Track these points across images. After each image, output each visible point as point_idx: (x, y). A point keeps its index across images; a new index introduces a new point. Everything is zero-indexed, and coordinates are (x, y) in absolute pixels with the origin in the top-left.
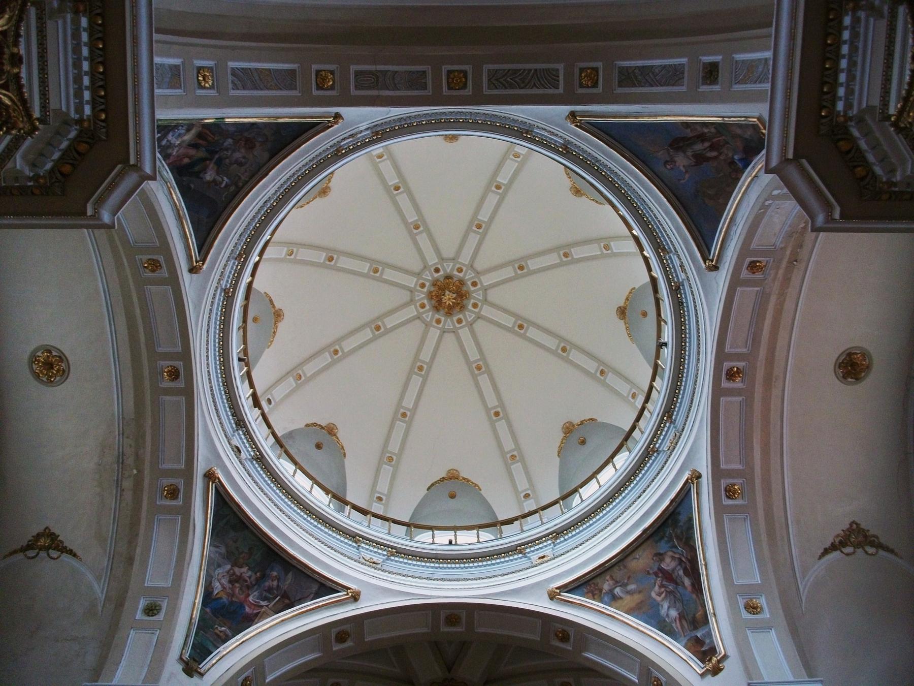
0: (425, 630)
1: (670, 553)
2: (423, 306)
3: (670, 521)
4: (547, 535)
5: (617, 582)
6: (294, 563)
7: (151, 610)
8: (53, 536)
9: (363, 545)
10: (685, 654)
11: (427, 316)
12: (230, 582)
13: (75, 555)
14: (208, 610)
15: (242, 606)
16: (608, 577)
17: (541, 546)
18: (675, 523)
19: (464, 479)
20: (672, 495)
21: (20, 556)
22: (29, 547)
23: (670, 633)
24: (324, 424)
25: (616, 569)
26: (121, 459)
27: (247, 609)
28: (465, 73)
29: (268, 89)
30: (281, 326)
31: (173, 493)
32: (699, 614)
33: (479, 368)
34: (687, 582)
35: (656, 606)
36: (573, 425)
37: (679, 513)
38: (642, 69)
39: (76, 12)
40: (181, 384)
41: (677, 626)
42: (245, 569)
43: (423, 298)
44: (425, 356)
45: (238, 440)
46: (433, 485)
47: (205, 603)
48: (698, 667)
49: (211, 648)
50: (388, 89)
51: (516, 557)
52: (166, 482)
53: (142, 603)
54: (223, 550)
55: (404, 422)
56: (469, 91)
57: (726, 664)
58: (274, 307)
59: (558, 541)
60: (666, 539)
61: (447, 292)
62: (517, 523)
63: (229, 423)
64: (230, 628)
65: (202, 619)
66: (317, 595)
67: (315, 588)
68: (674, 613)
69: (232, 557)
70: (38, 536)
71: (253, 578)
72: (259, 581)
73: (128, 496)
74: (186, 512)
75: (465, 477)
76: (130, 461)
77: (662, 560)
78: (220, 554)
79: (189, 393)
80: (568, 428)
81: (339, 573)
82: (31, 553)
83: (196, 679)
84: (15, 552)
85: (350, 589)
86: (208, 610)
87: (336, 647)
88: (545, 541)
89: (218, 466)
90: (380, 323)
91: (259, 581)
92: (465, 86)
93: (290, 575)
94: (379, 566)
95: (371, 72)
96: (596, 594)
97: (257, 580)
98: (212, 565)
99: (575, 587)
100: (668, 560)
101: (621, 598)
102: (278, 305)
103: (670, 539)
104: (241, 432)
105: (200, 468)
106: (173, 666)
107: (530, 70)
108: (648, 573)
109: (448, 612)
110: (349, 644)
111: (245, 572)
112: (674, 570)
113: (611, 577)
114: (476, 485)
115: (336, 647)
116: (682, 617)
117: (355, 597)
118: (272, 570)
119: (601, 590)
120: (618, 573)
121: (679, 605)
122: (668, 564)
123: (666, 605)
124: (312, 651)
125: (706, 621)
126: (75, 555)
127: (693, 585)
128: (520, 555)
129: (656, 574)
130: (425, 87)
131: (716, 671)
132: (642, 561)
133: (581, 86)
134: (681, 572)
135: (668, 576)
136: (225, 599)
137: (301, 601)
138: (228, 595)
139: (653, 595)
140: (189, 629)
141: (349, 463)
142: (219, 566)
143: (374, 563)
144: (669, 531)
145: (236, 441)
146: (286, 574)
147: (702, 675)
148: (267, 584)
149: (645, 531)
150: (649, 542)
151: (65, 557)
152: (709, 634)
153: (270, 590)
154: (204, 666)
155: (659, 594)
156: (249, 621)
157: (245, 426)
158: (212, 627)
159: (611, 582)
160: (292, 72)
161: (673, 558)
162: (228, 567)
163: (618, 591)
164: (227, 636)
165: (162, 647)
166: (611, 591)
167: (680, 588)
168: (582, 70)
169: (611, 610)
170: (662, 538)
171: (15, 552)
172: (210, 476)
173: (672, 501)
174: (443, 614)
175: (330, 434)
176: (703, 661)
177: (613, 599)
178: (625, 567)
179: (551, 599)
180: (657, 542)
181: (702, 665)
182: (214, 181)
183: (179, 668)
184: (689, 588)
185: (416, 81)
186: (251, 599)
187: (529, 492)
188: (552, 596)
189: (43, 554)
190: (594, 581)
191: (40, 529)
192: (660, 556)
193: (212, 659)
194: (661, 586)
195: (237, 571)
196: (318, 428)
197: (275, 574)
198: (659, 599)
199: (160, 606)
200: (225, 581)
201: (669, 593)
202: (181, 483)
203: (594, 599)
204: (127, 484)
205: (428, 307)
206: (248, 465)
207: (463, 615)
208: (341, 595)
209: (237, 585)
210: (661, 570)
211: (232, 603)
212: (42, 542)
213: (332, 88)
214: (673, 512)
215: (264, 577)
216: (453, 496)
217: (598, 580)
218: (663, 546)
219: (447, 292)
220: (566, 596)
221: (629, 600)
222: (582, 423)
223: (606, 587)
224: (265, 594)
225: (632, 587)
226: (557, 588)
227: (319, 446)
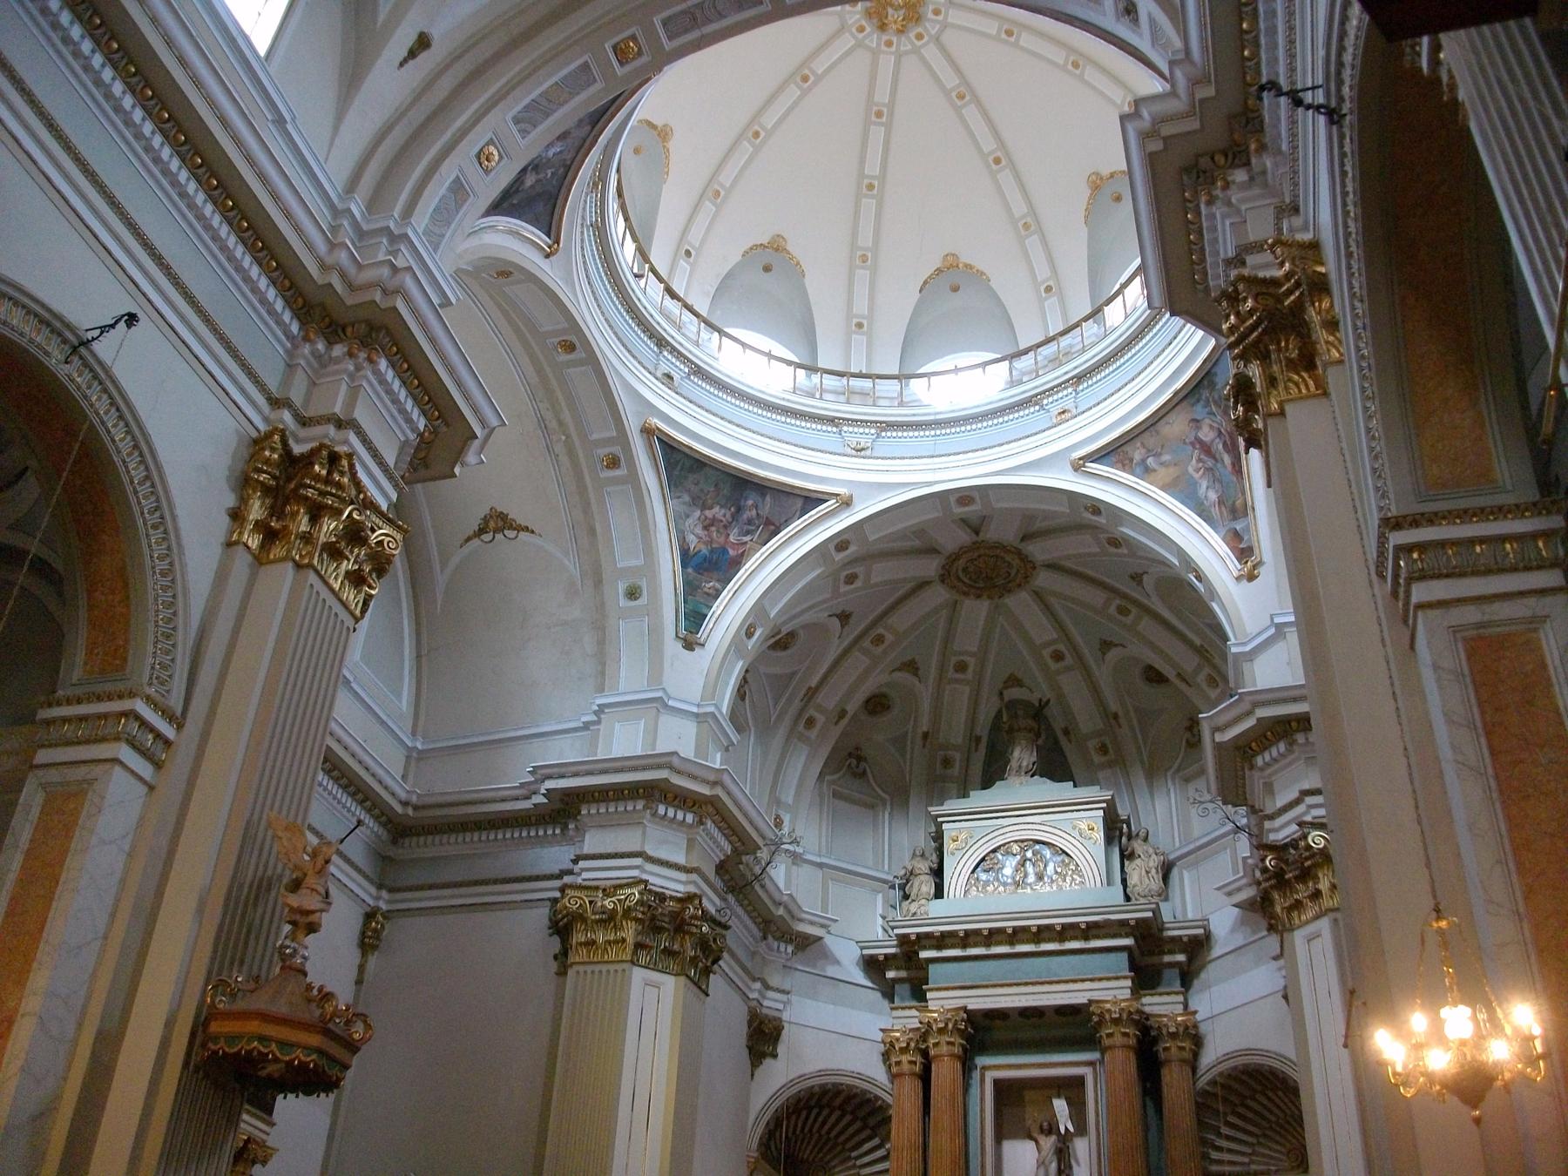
0: (936, 515)
1: (1207, 421)
2: (861, 29)
3: (1206, 383)
4: (1068, 381)
5: (1149, 451)
6: (768, 484)
7: (633, 594)
8: (502, 517)
9: (845, 428)
10: (1224, 549)
11: (872, 41)
12: (706, 528)
13: (533, 532)
14: (690, 570)
15: (724, 550)
16: (1139, 444)
17: (1060, 395)
18: (1212, 385)
19: (966, 266)
20: (1205, 354)
21: (476, 542)
22: (482, 531)
23: (1208, 519)
24: (765, 242)
25: (1147, 434)
26: (542, 423)
27: (732, 552)
29: (561, 105)
30: (671, 145)
31: (614, 463)
32: (1239, 502)
33: (961, 97)
34: (1227, 459)
35: (1194, 485)
36: (1101, 178)
37: (1216, 374)
39: (370, 360)
40: (579, 354)
41: (1215, 512)
42: (717, 509)
43: (859, 20)
44: (882, 96)
45: (668, 363)
46: (925, 283)
47: (684, 565)
48: (1234, 565)
49: (705, 611)
50: (711, 21)
51: (1032, 410)
52: (603, 452)
53: (622, 588)
54: (687, 498)
55: (873, 197)
57: (1262, 570)
58: (654, 127)
59: (1081, 387)
60: (1202, 403)
61: (890, 11)
62: (1031, 354)
63: (646, 347)
64: (718, 581)
65: (687, 583)
66: (804, 512)
67: (799, 503)
68: (1213, 496)
69: (699, 502)
70: (486, 520)
71: (728, 515)
72: (735, 517)
73: (564, 459)
74: (634, 478)
75: (968, 262)
76: (553, 424)
77: (1199, 428)
78: (684, 503)
79: (592, 361)
80: (1094, 182)
81: (822, 480)
82: (487, 537)
83: (698, 649)
84: (468, 539)
85: (838, 495)
86: (690, 570)
87: (839, 557)
88: (1065, 388)
89: (653, 416)
90: (806, 71)
91: (735, 517)
93: (768, 498)
94: (868, 453)
95: (683, 12)
96: (1126, 464)
97: (733, 516)
98: (679, 520)
99: (1101, 456)
100: (1206, 429)
101: (1155, 471)
102: (659, 122)
103: (1207, 404)
104: (665, 353)
105: (633, 425)
106: (673, 647)
108: (1185, 443)
109: (957, 495)
110: (852, 549)
111: (718, 512)
112: (1213, 441)
113: (1143, 445)
114: (983, 273)
115: (839, 557)
116: (1221, 502)
117: (847, 503)
118: (746, 499)
119: (1131, 460)
120: (1150, 439)
121: (1217, 485)
122: (1206, 434)
123: (1204, 484)
124: (813, 570)
125: (1246, 515)
126: (533, 532)
127: (1233, 465)
128: (1037, 408)
129: (1192, 444)
131: (1251, 577)
132: (1177, 425)
134: (1220, 446)
135: (1206, 449)
136: (705, 550)
137: (787, 523)
138: (706, 543)
139: (1190, 470)
140: (677, 602)
141: (812, 283)
142: (688, 516)
143: (863, 449)
144: (1205, 393)
145: (664, 367)
146: (763, 495)
147: (1238, 579)
148: (745, 516)
149: (1176, 393)
150: (1184, 404)
151: (522, 535)
152: (1247, 529)
153: (750, 522)
154: (702, 634)
155: (1197, 470)
156: (737, 563)
157: (668, 343)
158: (699, 587)
159: (1143, 451)
160: (585, 66)
161: (1211, 427)
162: (698, 513)
163: (1150, 461)
164: (717, 590)
165: (655, 632)
166: (1144, 461)
167: (1219, 465)
169: (1143, 485)
170: (1198, 401)
171: (468, 539)
172: (648, 431)
173: (1205, 361)
174: (952, 499)
175: (777, 250)
176: (1239, 560)
177: (1146, 472)
178: (1157, 432)
179: (1076, 470)
180: (1193, 405)
181: (1239, 567)
182: (538, 181)
183: (679, 645)
184: (1229, 467)
186: (732, 538)
187: (1051, 283)
188: (1078, 466)
189: (499, 536)
190: (1124, 448)
191: (484, 511)
192: (1196, 422)
193: (708, 624)
194: (1200, 460)
195: (709, 513)
197: (750, 502)
198: (1196, 476)
199: (640, 587)
200: (699, 531)
201: (1209, 470)
202: (617, 450)
203: (1124, 471)
204: (559, 448)
205: (868, 29)
206: (687, 384)
207: (976, 495)
208: (831, 504)
209: (713, 529)
210: (1201, 442)
211: (712, 551)
212: (492, 524)
213: (640, 53)
214: (1208, 373)
215: (739, 510)
216: (955, 289)
217: (1127, 448)
218: (1199, 411)
219: (890, 11)
220: (1094, 467)
221: (1164, 474)
222: (1112, 175)
223: (1137, 457)
224: (745, 527)
225: (1166, 457)
226: (1080, 459)
227: (767, 269)
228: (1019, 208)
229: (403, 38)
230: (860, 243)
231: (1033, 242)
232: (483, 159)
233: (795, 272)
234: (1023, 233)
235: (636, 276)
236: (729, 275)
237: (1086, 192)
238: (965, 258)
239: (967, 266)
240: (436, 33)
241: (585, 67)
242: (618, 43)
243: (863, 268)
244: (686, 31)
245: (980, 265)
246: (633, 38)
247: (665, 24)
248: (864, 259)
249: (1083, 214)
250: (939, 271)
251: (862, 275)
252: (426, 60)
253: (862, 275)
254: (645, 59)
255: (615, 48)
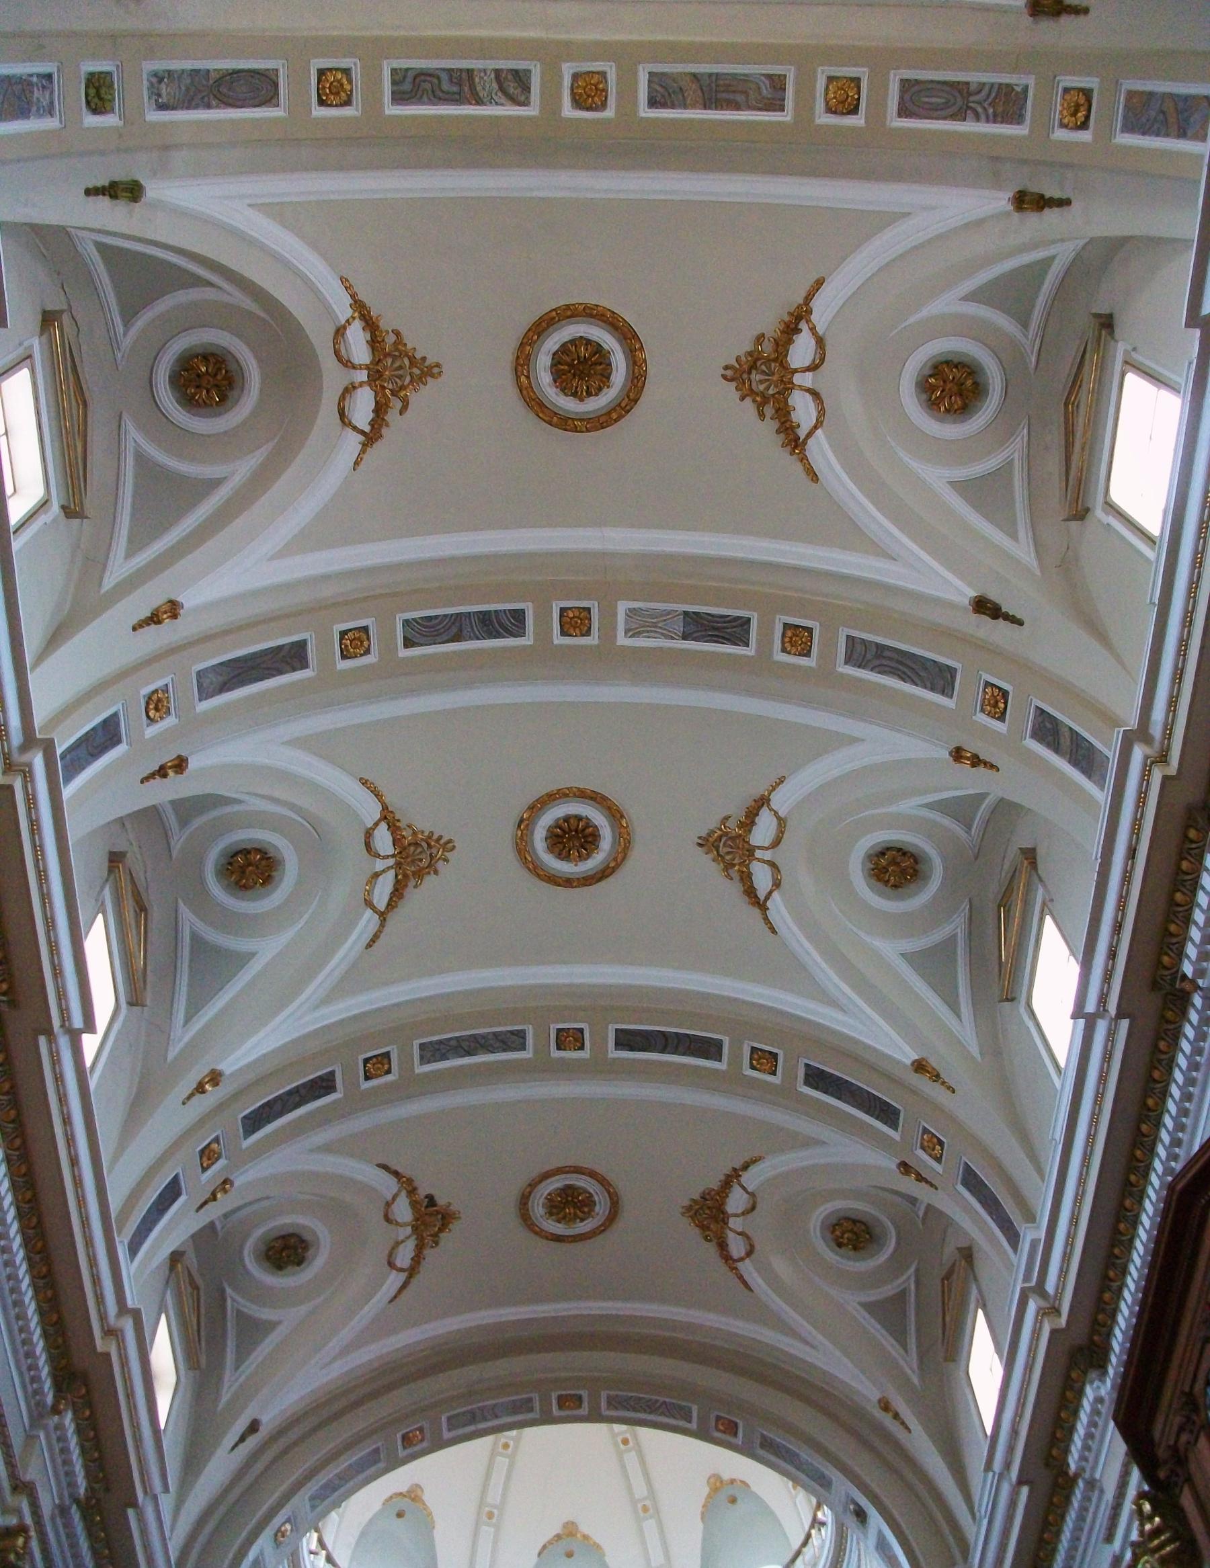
28: (580, 1398)
36: (722, 1482)
38: (788, 1450)
46: (544, 1547)
56: (584, 1410)
75: (586, 1533)
92: (580, 1406)
107: (657, 1401)
114: (598, 1547)
130: (531, 1410)
133: (718, 1430)
168: (718, 1418)
175: (413, 1500)
185: (524, 1406)
196: (399, 1498)
213: (422, 1440)
216: (570, 1555)
222: (732, 1481)
227: (400, 1515)
228: (640, 1490)
229: (241, 1425)
230: (489, 1500)
231: (650, 1525)
232: (280, 1534)
233: (427, 1524)
234: (642, 1514)
235: (311, 1552)
236: (371, 1521)
237: (706, 1490)
238: (584, 1528)
239: (586, 1537)
240: (265, 1419)
241: (377, 1451)
242: (408, 1433)
243: (488, 1525)
244: (465, 1425)
245: (597, 1538)
246: (421, 1429)
247: (449, 1419)
248: (490, 1515)
249: (700, 1509)
250: (558, 1537)
251: (487, 1531)
252: (252, 1442)
253: (487, 1531)
254: (425, 1444)
255: (405, 1438)
